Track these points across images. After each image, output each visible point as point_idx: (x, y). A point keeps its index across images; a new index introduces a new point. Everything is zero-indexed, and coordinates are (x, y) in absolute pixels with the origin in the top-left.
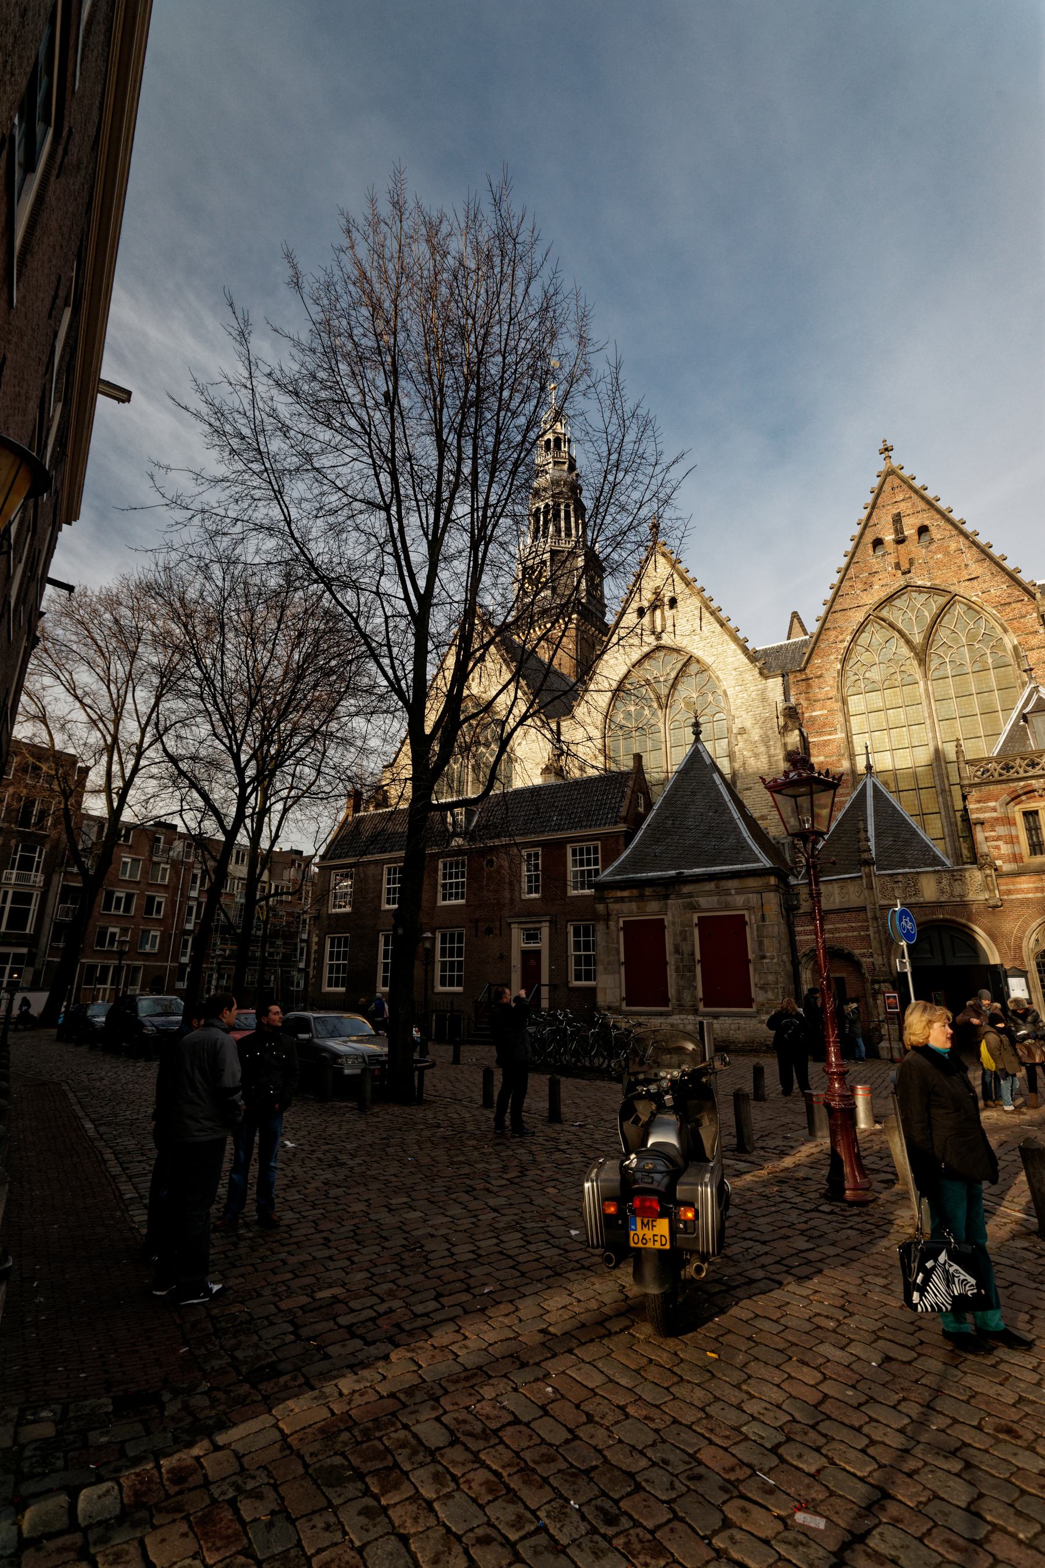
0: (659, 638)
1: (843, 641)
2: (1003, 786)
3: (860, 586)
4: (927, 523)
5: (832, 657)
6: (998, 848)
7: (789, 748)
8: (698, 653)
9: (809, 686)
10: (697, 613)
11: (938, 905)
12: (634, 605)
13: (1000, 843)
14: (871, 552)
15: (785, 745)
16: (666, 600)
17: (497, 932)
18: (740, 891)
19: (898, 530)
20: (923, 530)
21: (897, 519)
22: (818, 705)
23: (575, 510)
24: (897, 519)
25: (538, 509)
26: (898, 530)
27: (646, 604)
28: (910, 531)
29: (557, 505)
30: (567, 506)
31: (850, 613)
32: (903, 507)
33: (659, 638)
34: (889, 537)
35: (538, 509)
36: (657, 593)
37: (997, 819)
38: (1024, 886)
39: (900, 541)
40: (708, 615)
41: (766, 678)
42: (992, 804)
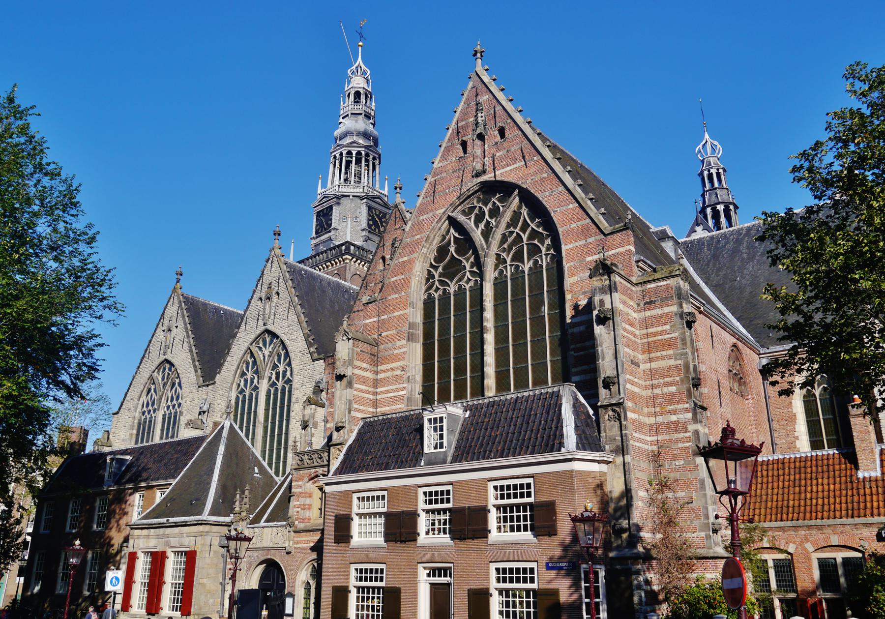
7: (306, 419)
10: (288, 305)
11: (268, 549)
12: (257, 295)
13: (299, 509)
15: (304, 415)
16: (274, 292)
18: (189, 535)
23: (367, 155)
27: (263, 297)
29: (349, 153)
30: (359, 153)
36: (269, 288)
38: (304, 539)
41: (314, 361)
42: (300, 483)
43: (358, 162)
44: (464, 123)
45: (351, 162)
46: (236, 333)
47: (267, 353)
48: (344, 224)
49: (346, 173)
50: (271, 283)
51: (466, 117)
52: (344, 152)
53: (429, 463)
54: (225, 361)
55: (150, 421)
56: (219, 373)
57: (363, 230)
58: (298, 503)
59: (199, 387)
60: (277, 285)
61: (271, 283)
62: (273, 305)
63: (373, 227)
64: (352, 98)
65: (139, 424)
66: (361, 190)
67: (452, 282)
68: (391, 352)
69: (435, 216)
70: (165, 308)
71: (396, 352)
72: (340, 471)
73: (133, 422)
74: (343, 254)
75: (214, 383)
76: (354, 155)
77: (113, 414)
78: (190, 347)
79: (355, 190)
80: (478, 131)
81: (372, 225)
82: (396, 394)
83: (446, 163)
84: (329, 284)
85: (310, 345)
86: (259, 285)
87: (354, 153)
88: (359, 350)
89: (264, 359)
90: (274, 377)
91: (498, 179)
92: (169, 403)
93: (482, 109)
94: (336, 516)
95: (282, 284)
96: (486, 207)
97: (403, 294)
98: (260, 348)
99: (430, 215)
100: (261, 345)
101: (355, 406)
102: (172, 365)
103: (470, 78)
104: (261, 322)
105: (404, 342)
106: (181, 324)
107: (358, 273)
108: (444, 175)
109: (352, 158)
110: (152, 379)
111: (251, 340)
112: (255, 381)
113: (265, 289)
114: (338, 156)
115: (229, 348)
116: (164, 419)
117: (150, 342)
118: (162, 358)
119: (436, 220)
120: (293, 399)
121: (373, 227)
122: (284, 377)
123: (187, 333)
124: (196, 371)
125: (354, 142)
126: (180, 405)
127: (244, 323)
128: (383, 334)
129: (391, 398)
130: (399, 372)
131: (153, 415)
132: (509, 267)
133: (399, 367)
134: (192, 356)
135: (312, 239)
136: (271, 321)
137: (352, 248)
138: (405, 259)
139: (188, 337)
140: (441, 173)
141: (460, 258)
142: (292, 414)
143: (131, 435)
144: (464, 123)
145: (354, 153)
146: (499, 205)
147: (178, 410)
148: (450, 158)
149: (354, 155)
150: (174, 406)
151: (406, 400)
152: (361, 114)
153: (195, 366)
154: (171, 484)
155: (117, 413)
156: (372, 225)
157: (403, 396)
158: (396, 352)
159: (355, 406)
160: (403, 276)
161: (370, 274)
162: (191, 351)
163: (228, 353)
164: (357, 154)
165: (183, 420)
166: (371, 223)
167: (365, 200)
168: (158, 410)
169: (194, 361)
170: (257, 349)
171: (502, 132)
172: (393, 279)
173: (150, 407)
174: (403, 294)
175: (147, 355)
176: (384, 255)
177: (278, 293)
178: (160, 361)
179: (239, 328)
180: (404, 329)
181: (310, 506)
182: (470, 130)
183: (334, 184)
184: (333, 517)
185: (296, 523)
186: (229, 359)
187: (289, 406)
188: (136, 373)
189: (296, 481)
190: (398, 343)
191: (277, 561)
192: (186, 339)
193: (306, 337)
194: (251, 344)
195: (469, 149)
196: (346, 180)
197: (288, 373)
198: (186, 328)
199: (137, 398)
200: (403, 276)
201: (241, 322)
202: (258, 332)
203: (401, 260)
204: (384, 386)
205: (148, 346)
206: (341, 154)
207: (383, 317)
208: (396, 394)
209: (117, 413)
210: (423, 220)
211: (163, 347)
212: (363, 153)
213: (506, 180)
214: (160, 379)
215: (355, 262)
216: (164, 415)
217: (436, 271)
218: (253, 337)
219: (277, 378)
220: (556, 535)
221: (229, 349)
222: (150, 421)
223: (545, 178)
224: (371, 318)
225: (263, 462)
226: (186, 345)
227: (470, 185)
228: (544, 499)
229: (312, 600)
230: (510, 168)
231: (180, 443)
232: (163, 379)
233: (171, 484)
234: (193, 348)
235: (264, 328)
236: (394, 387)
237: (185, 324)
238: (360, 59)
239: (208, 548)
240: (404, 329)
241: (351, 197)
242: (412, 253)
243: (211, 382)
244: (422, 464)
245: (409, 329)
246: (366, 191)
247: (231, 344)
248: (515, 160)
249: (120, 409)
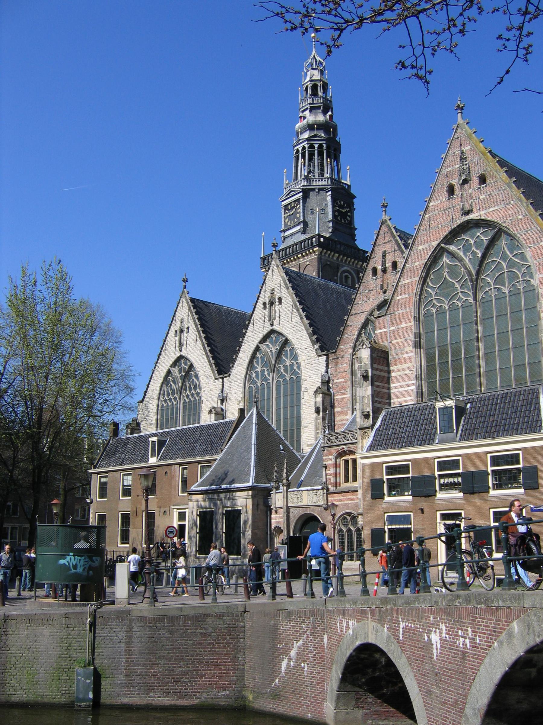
0: (272, 325)
1: (353, 335)
2: (335, 448)
3: (365, 299)
4: (396, 259)
5: (348, 345)
6: (330, 479)
7: (318, 406)
8: (290, 337)
9: (337, 363)
11: (308, 507)
14: (371, 276)
15: (316, 402)
17: (168, 513)
19: (384, 264)
20: (395, 265)
21: (384, 256)
22: (340, 375)
23: (328, 147)
24: (384, 256)
25: (298, 151)
26: (384, 264)
27: (267, 301)
28: (389, 265)
29: (312, 146)
30: (321, 146)
31: (358, 316)
32: (388, 247)
33: (272, 325)
34: (379, 268)
35: (298, 151)
37: (331, 464)
39: (384, 271)
40: (295, 311)
41: (319, 356)
42: (330, 457)
43: (321, 154)
44: (450, 169)
45: (314, 155)
46: (246, 333)
47: (274, 350)
48: (312, 216)
49: (309, 165)
50: (273, 290)
51: (452, 164)
52: (306, 146)
53: (441, 442)
54: (237, 357)
55: (172, 409)
56: (232, 367)
57: (329, 221)
58: (329, 472)
59: (216, 379)
60: (279, 291)
61: (273, 290)
62: (277, 308)
63: (339, 218)
64: (310, 91)
65: (162, 411)
66: (326, 183)
67: (446, 299)
68: (400, 356)
69: (430, 246)
70: (176, 311)
71: (404, 356)
72: (371, 448)
73: (158, 409)
74: (314, 247)
75: (229, 376)
76: (316, 149)
77: (139, 402)
78: (203, 345)
79: (320, 184)
80: (463, 177)
81: (338, 216)
82: (406, 389)
83: (437, 202)
84: (320, 285)
85: (313, 343)
86: (263, 291)
87: (316, 146)
88: (376, 356)
89: (272, 354)
90: (282, 370)
91: (483, 218)
92: (188, 393)
93: (466, 158)
94: (372, 480)
95: (284, 290)
96: (473, 240)
97: (408, 310)
98: (268, 346)
99: (426, 246)
100: (268, 343)
101: (376, 399)
102: (186, 358)
103: (461, 145)
104: (268, 324)
105: (411, 348)
106: (192, 327)
107: (328, 263)
108: (436, 212)
109: (314, 151)
110: (169, 372)
111: (259, 339)
112: (266, 373)
113: (268, 294)
114: (300, 149)
115: (240, 345)
116: (184, 407)
117: (165, 341)
118: (178, 354)
119: (432, 250)
120: (303, 389)
121: (339, 218)
122: (291, 371)
123: (199, 333)
124: (211, 366)
125: (315, 136)
126: (198, 394)
127: (251, 324)
128: (393, 342)
129: (402, 392)
130: (408, 372)
131: (175, 403)
132: (493, 290)
133: (408, 368)
134: (206, 353)
135: (281, 231)
136: (275, 323)
137: (322, 240)
138: (407, 281)
139: (200, 336)
140: (434, 211)
141: (454, 281)
142: (303, 401)
143: (157, 420)
144: (450, 169)
145: (316, 146)
146: (484, 238)
147: (197, 398)
148: (441, 198)
149: (316, 149)
150: (193, 395)
151: (415, 393)
152: (320, 106)
153: (209, 361)
154: (215, 460)
155: (142, 401)
156: (338, 216)
157: (412, 390)
158: (404, 356)
159: (376, 399)
160: (407, 296)
161: (364, 282)
162: (204, 348)
163: (239, 350)
164: (318, 148)
165: (205, 407)
166: (337, 214)
167: (330, 193)
168: (180, 399)
169: (208, 357)
170: (264, 346)
171: (483, 180)
172: (398, 298)
173: (171, 396)
174: (408, 310)
175: (163, 352)
176: (376, 266)
177: (280, 299)
178: (176, 357)
179: (247, 329)
180: (410, 338)
181: (340, 473)
182: (456, 176)
183: (299, 178)
184: (369, 481)
185: (329, 487)
186: (240, 355)
187: (299, 394)
188: (155, 368)
189: (326, 456)
190: (406, 349)
191: (316, 515)
192: (198, 338)
193: (310, 336)
194: (260, 343)
195: (457, 191)
196: (309, 172)
197: (295, 367)
198: (197, 329)
199: (158, 389)
200: (407, 296)
201: (249, 323)
202: (265, 332)
203: (404, 282)
204: (396, 383)
205: (164, 344)
206: (304, 148)
207: (392, 328)
208: (406, 389)
209: (142, 401)
210: (421, 250)
211: (177, 345)
212: (325, 145)
213: (489, 219)
214: (178, 373)
215: (326, 253)
216: (185, 402)
217: (433, 291)
218: (261, 336)
219: (286, 371)
220: (538, 489)
221: (240, 347)
222: (172, 409)
223: (521, 219)
224: (382, 329)
225: (285, 441)
226: (199, 344)
227: (459, 222)
228: (528, 465)
229: (346, 544)
230: (491, 210)
231: (209, 427)
232: (180, 371)
233: (215, 460)
234: (206, 346)
235: (271, 328)
236: (404, 383)
237: (196, 326)
238: (314, 52)
239: (256, 508)
240: (410, 338)
241: (317, 190)
242: (413, 276)
243: (228, 374)
244: (437, 441)
245: (415, 338)
246: (329, 183)
247: (242, 342)
248: (496, 203)
249: (144, 398)
